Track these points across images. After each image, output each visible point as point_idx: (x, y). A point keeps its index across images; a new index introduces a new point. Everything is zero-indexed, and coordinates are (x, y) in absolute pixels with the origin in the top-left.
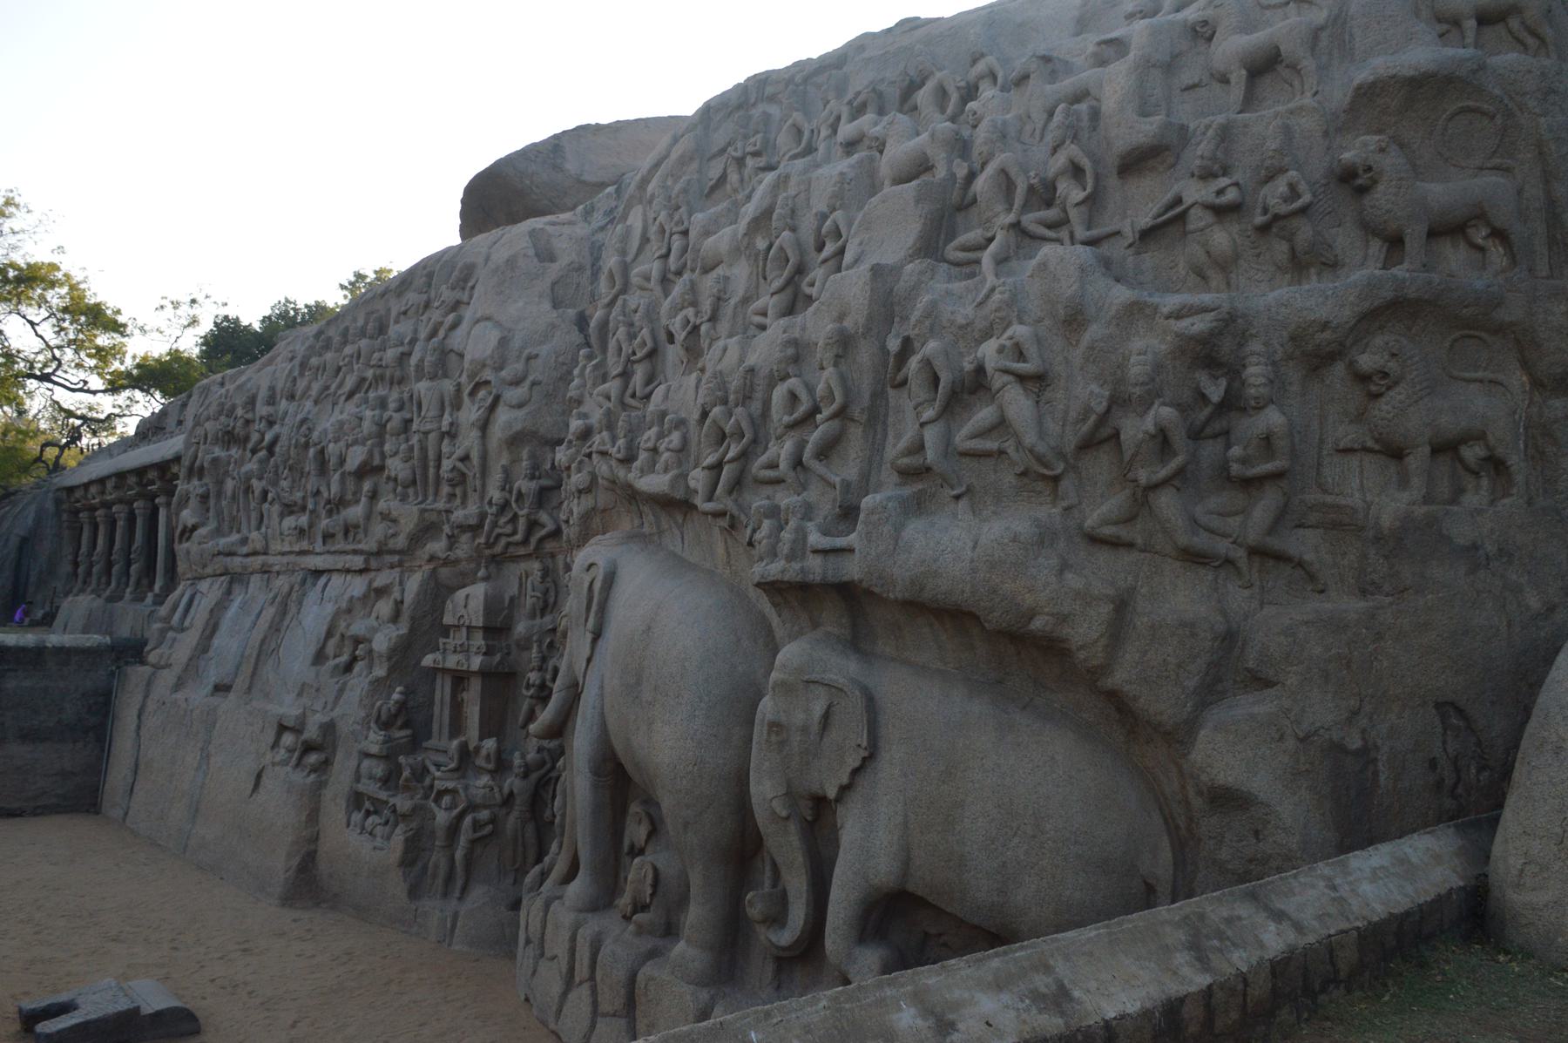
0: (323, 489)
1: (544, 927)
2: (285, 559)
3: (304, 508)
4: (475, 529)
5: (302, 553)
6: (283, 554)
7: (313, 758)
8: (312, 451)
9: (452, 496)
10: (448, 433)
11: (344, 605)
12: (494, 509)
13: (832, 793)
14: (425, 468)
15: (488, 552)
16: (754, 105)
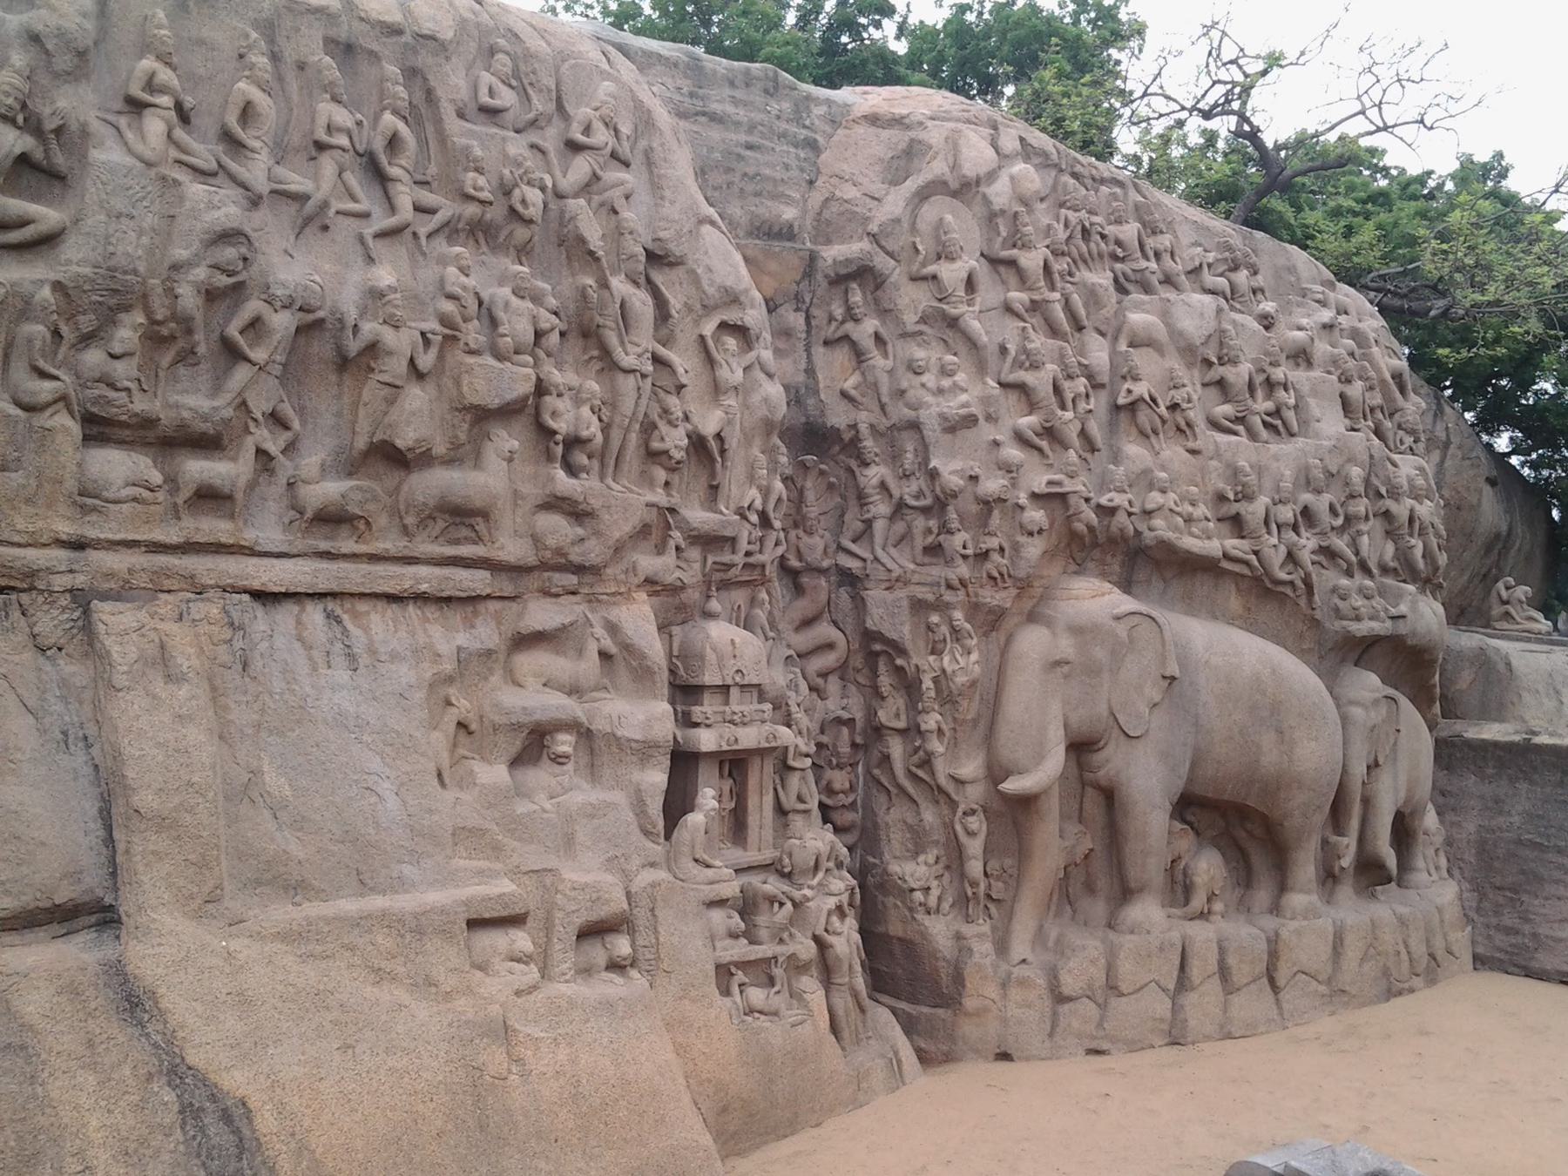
0: (287, 410)
1: (1110, 969)
2: (117, 561)
3: (208, 443)
4: (709, 541)
5: (188, 548)
6: (78, 545)
7: (622, 946)
8: (282, 322)
9: (667, 484)
10: (680, 387)
11: (448, 667)
12: (754, 518)
13: (1381, 761)
14: (627, 430)
15: (717, 576)
16: (1062, 171)
